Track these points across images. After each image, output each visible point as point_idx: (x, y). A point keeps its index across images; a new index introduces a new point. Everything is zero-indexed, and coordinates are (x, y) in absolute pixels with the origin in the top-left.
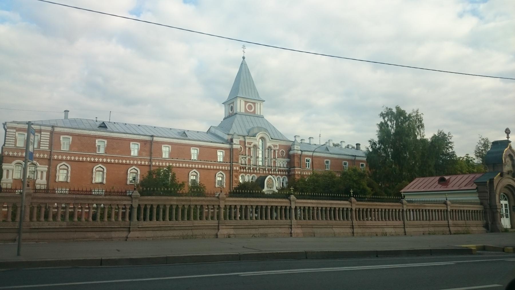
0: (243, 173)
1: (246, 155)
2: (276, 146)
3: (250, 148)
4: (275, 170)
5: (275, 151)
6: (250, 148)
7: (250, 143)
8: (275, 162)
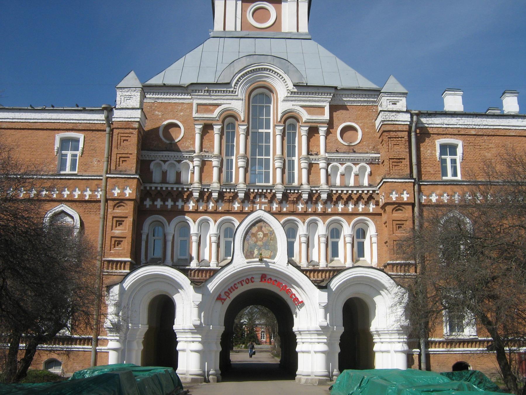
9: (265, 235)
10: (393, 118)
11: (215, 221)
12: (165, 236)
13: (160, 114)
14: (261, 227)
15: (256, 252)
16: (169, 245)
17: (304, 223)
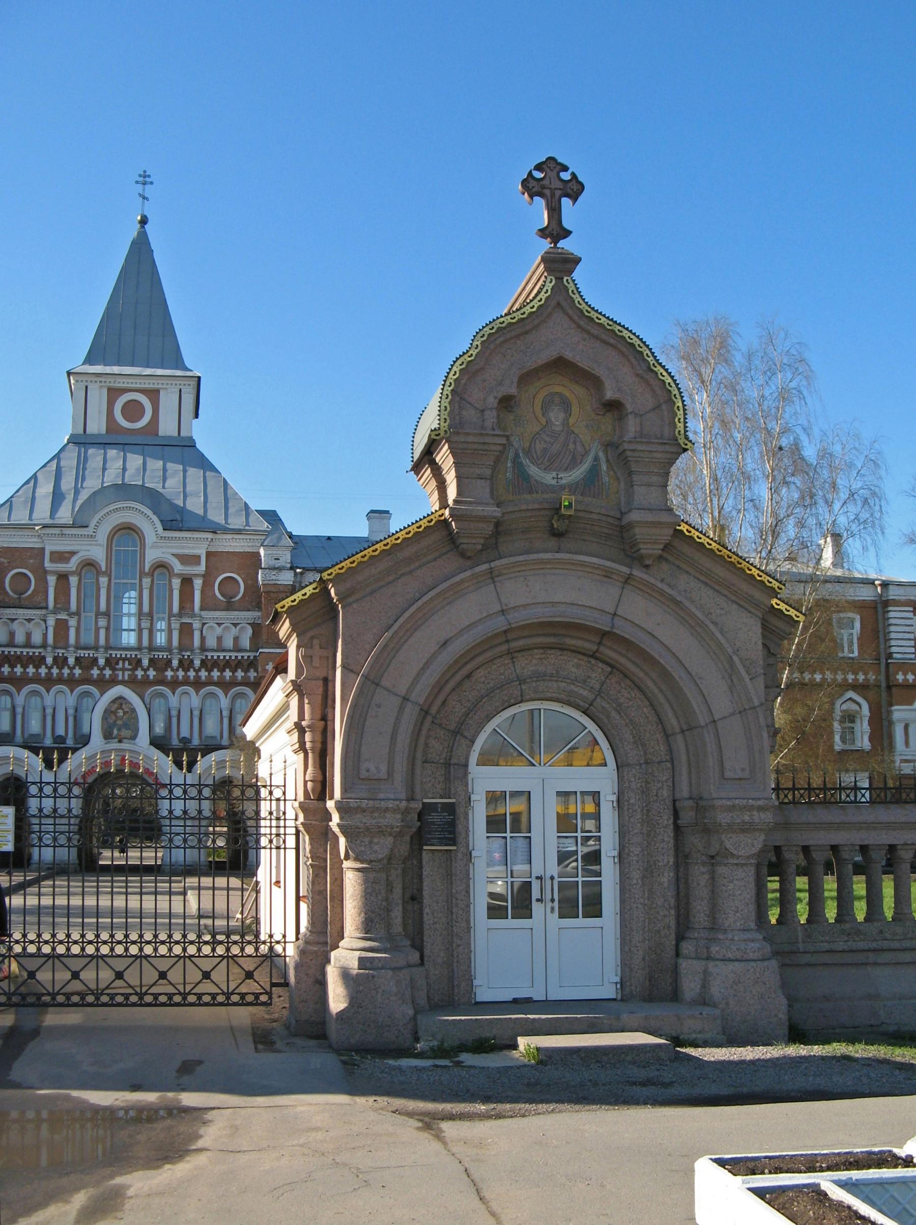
0: (37, 680)
1: (46, 608)
2: (195, 559)
3: (63, 577)
4: (186, 665)
5: (187, 581)
6: (63, 577)
7: (61, 557)
8: (186, 630)
9: (125, 713)
10: (274, 577)
11: (72, 691)
12: (14, 708)
13: (5, 561)
14: (121, 704)
15: (115, 732)
16: (19, 718)
17: (174, 694)
